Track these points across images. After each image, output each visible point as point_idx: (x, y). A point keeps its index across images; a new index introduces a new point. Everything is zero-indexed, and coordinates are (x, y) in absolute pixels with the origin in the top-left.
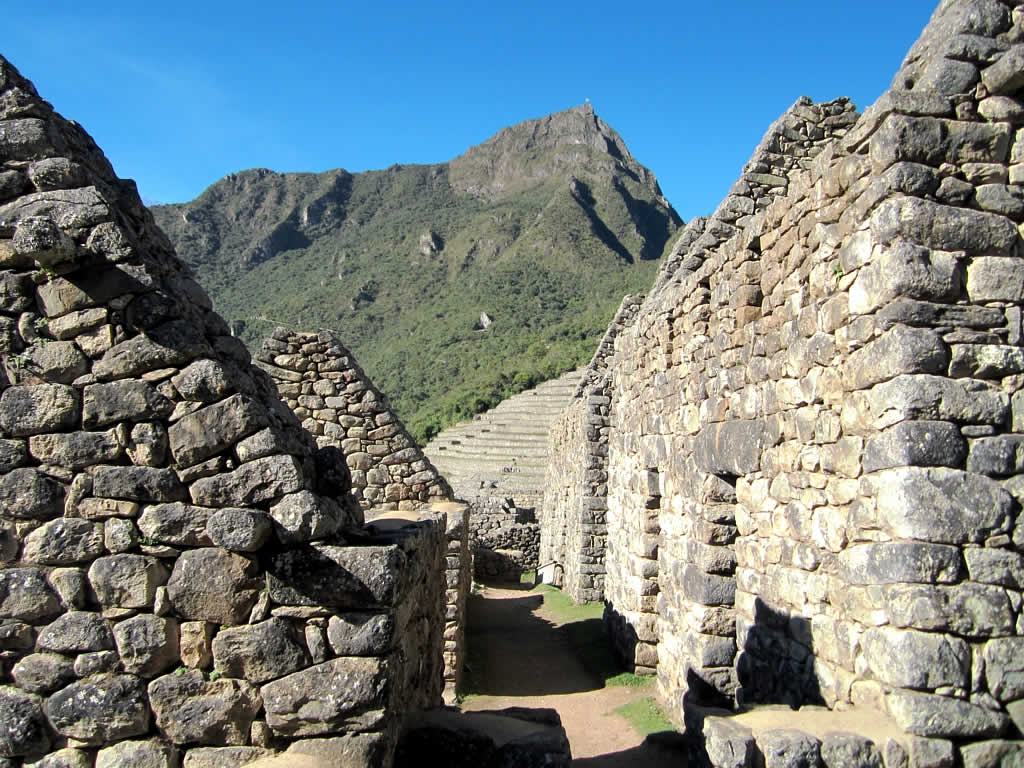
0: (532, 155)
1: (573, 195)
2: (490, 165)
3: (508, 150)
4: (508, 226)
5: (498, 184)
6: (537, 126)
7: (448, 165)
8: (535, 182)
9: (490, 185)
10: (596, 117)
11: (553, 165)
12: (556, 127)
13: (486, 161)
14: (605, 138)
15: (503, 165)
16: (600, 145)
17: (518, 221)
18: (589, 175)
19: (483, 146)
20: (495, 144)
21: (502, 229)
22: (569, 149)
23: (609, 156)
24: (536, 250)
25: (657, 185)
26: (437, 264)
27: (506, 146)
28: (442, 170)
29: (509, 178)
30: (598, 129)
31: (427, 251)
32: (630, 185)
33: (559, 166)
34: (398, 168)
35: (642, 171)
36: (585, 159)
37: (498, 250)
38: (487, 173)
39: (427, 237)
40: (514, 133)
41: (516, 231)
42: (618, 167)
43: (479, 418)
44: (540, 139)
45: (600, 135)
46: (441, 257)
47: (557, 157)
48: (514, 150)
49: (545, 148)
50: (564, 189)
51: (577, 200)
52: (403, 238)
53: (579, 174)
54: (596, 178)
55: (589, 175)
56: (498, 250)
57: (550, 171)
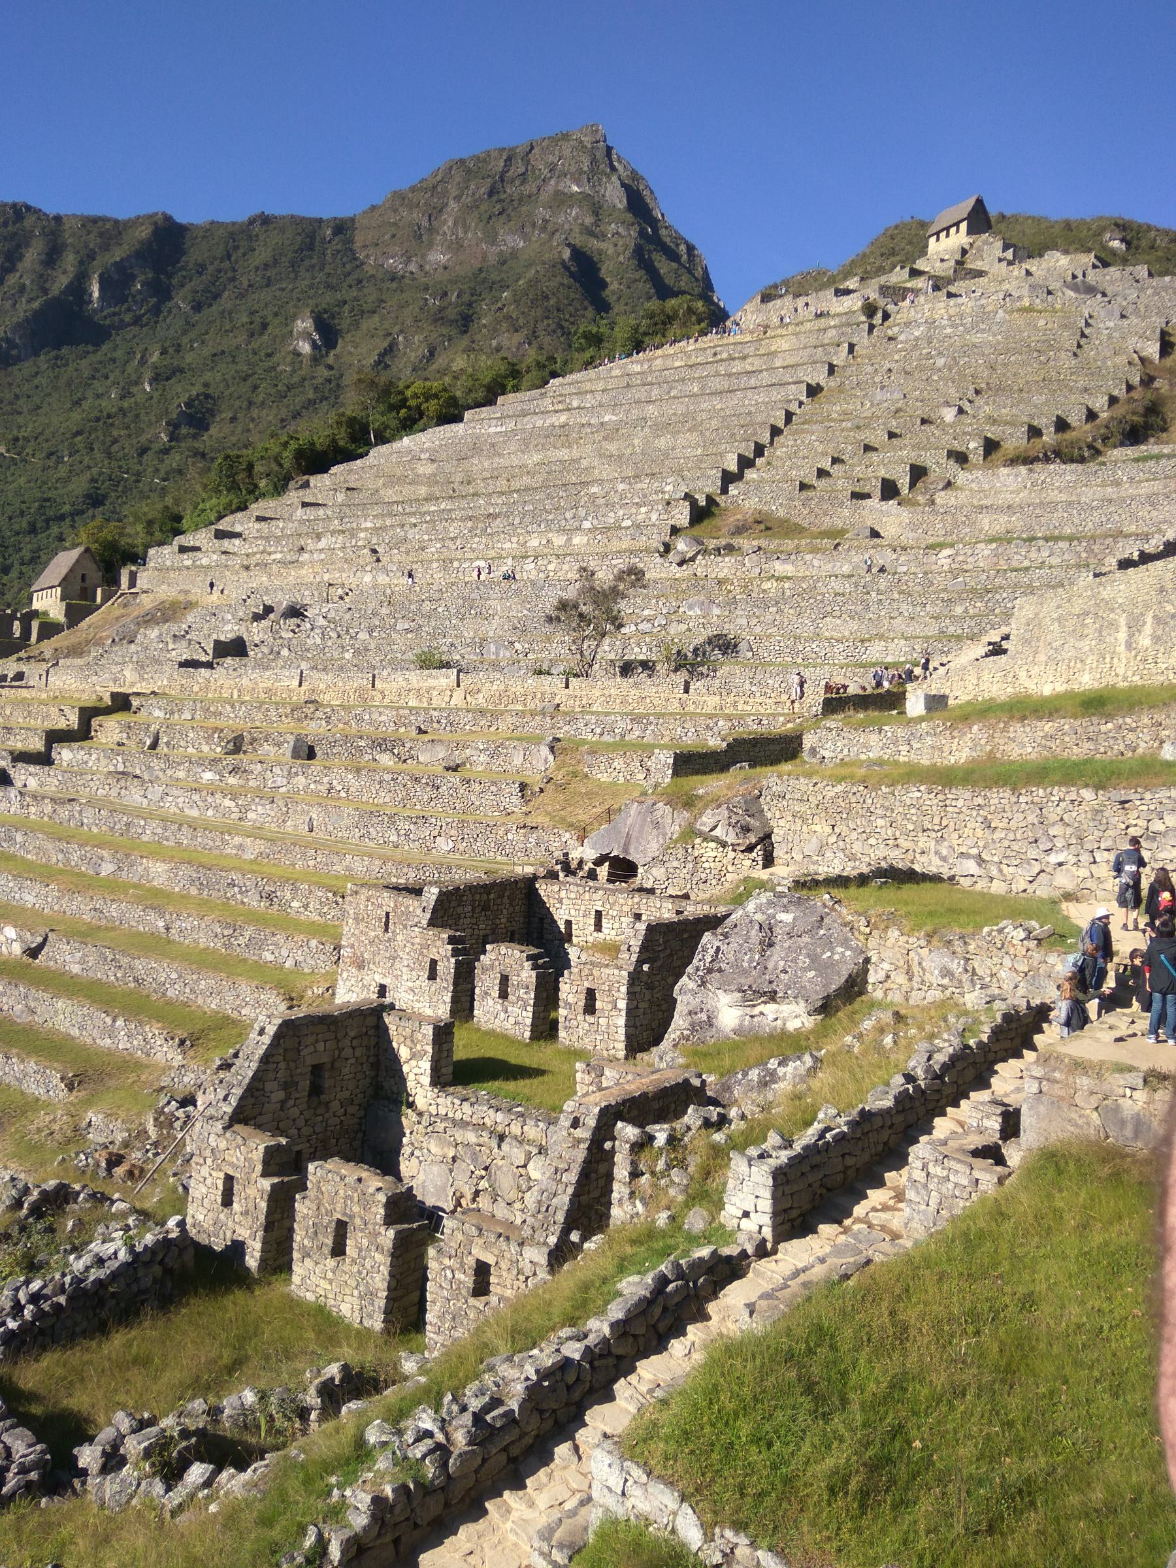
0: (498, 206)
1: (567, 268)
2: (425, 223)
3: (457, 198)
4: (452, 313)
5: (438, 257)
6: (509, 159)
7: (353, 220)
8: (501, 253)
9: (424, 256)
10: (609, 150)
11: (534, 225)
12: (540, 164)
13: (418, 216)
14: (623, 185)
15: (447, 223)
16: (614, 195)
17: (470, 305)
18: (595, 244)
19: (413, 189)
20: (435, 187)
21: (438, 318)
22: (562, 200)
23: (629, 217)
24: (498, 349)
25: (706, 271)
26: (322, 372)
27: (454, 192)
28: (342, 228)
29: (456, 247)
30: (613, 169)
31: (305, 348)
32: (664, 267)
33: (543, 229)
34: (266, 220)
35: (683, 247)
36: (589, 220)
37: (432, 353)
38: (421, 237)
39: (305, 324)
40: (469, 169)
41: (465, 322)
42: (642, 233)
43: (306, 485)
44: (512, 181)
45: (614, 179)
46: (330, 360)
47: (541, 212)
48: (468, 200)
49: (521, 200)
50: (554, 255)
51: (572, 275)
52: (265, 326)
53: (578, 239)
54: (607, 247)
55: (595, 244)
56: (432, 353)
57: (525, 237)
